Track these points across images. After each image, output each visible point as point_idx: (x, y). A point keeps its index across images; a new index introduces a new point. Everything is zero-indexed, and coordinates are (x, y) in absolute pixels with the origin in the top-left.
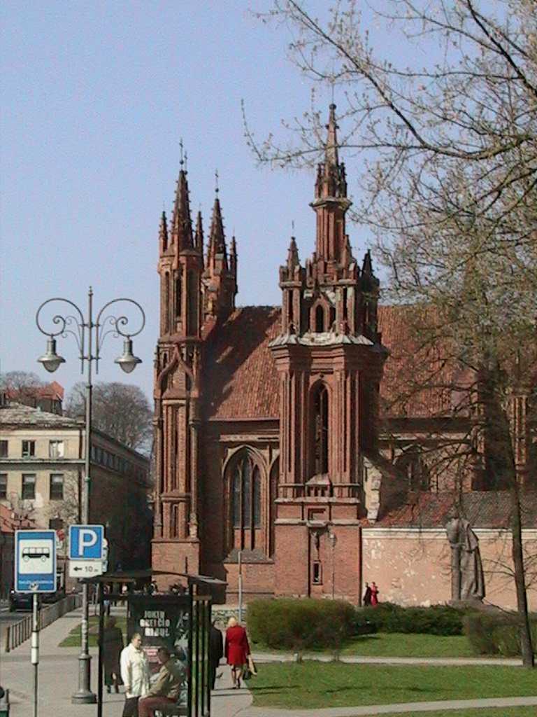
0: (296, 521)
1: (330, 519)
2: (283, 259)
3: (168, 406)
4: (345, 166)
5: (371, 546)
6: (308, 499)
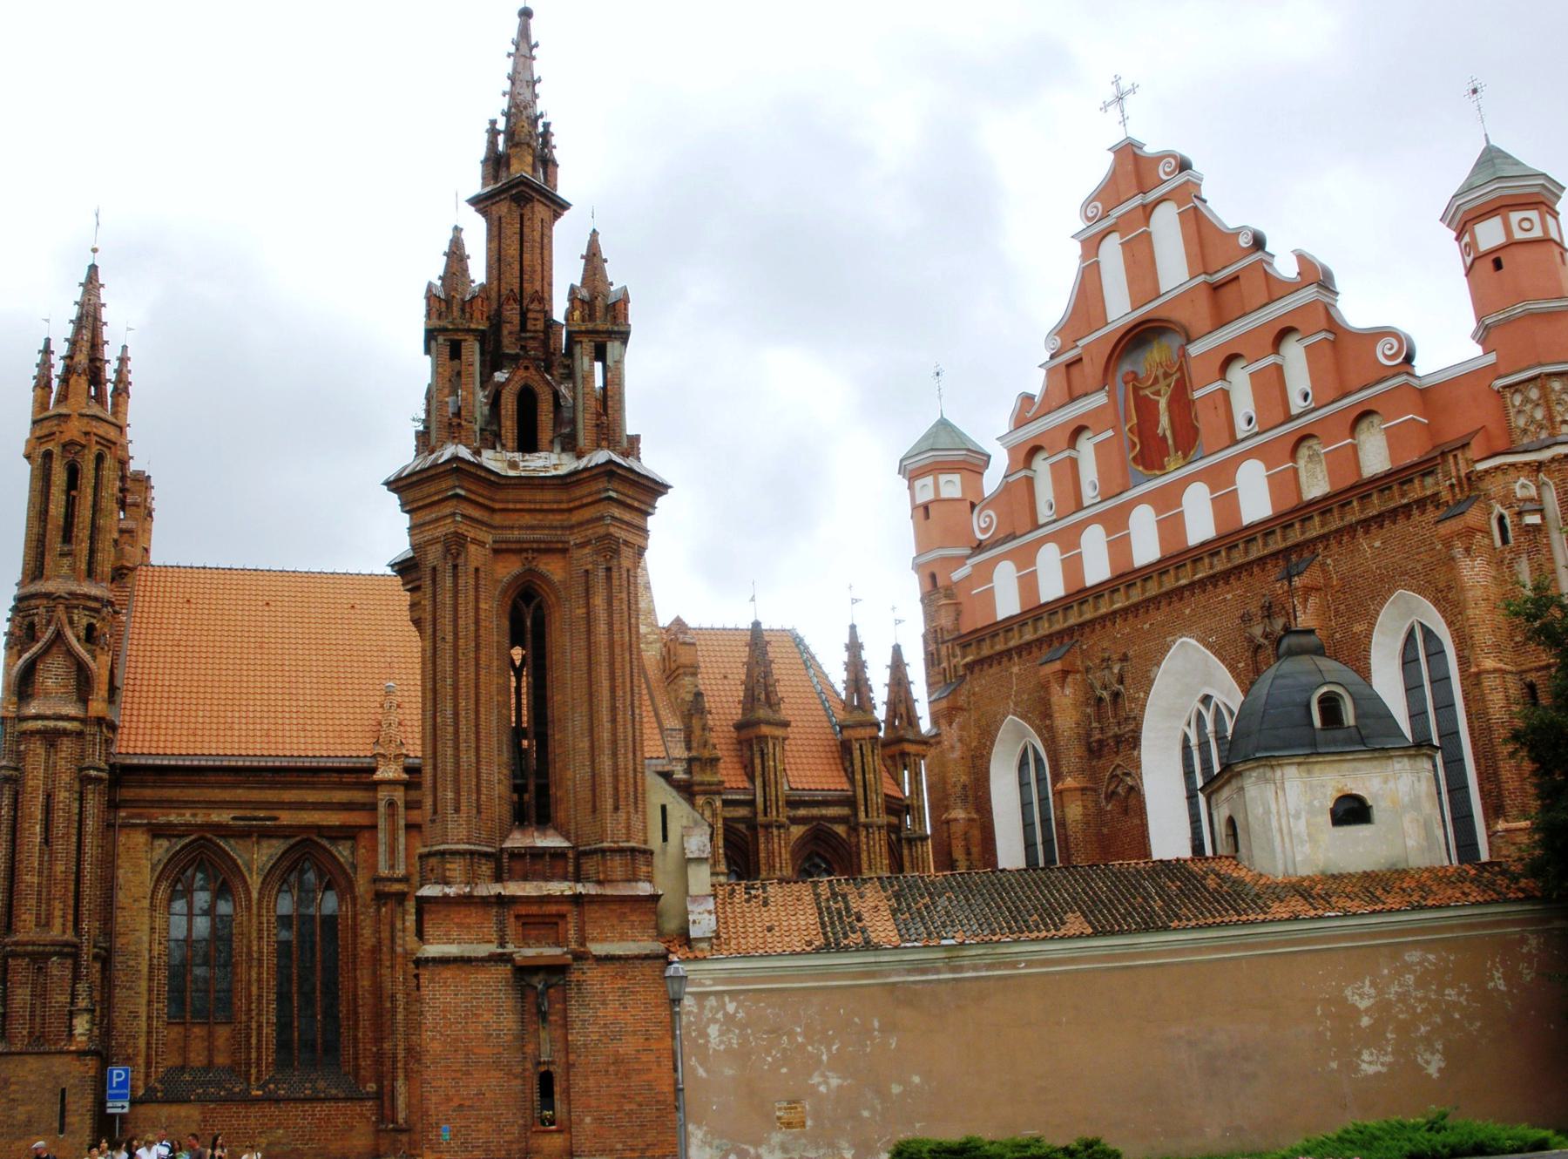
0: (483, 950)
1: (583, 944)
2: (435, 269)
3: (33, 733)
4: (552, 129)
5: (708, 1014)
6: (513, 889)
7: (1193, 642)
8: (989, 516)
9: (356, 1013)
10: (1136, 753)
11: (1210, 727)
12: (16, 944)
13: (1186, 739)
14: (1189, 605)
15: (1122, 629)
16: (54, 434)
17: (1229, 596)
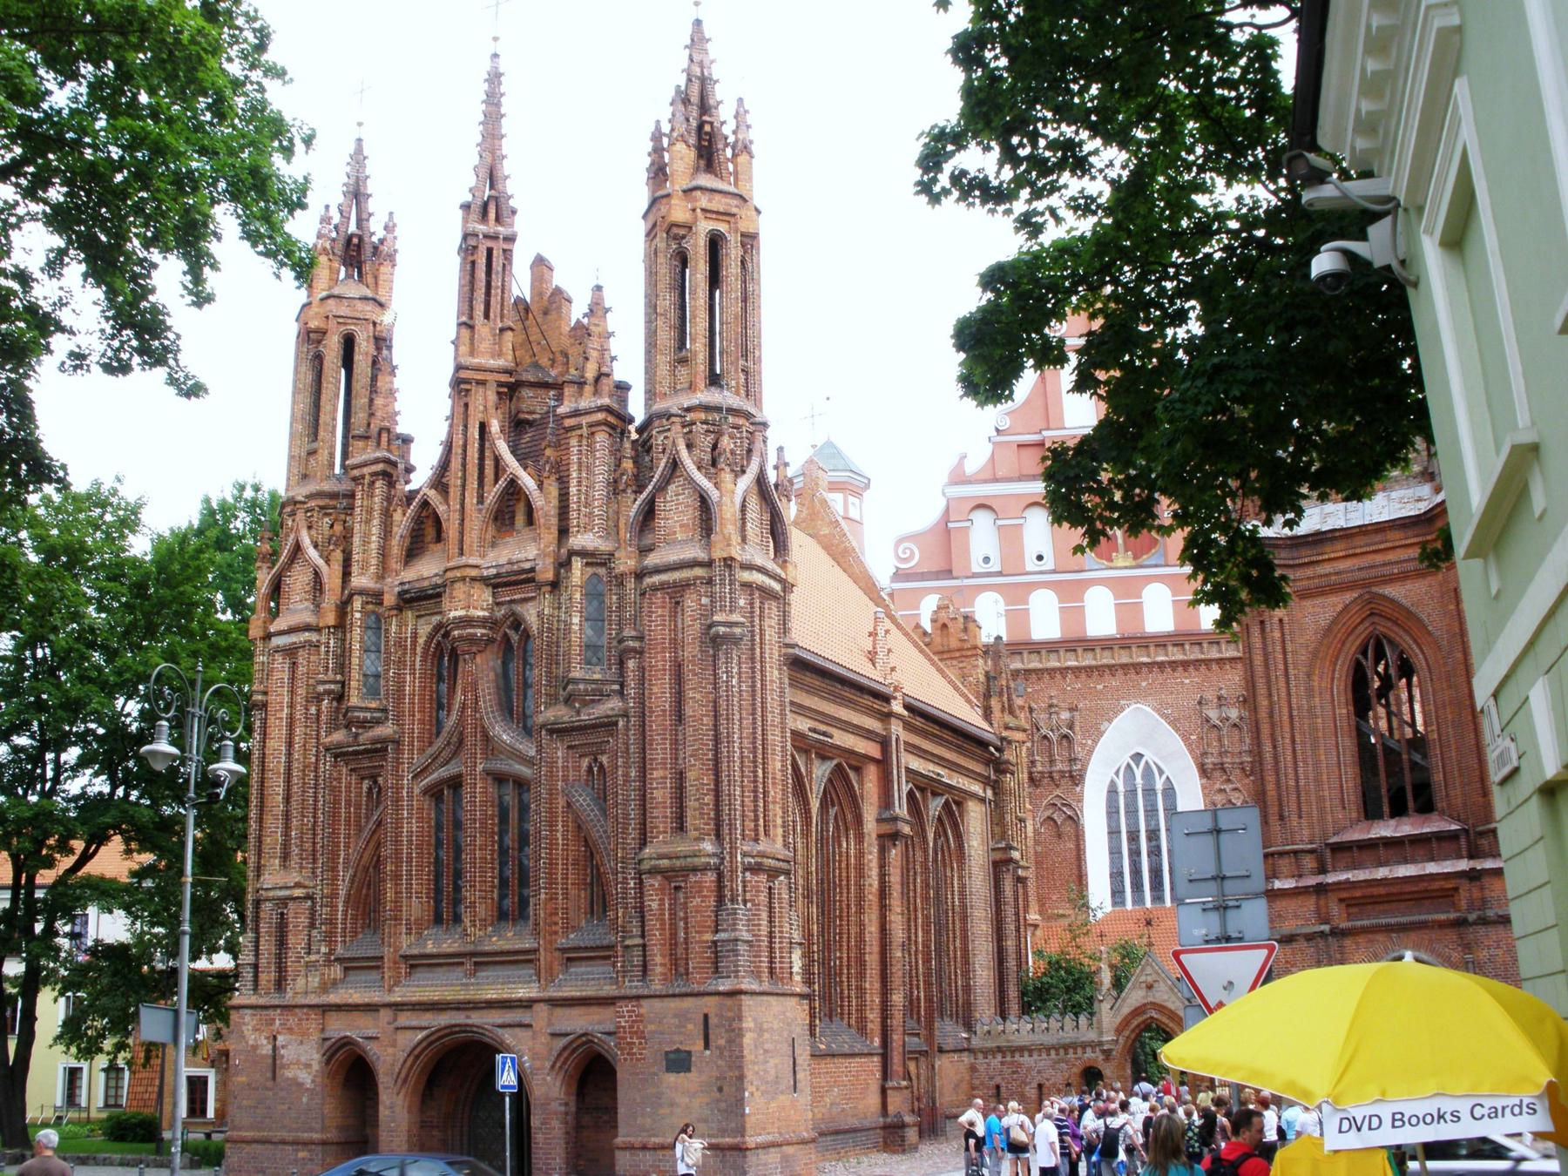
7: (1148, 709)
8: (912, 553)
9: (861, 963)
10: (1078, 789)
11: (1139, 781)
12: (763, 855)
13: (1113, 785)
14: (1145, 680)
15: (1072, 684)
16: (734, 215)
17: (1187, 681)
